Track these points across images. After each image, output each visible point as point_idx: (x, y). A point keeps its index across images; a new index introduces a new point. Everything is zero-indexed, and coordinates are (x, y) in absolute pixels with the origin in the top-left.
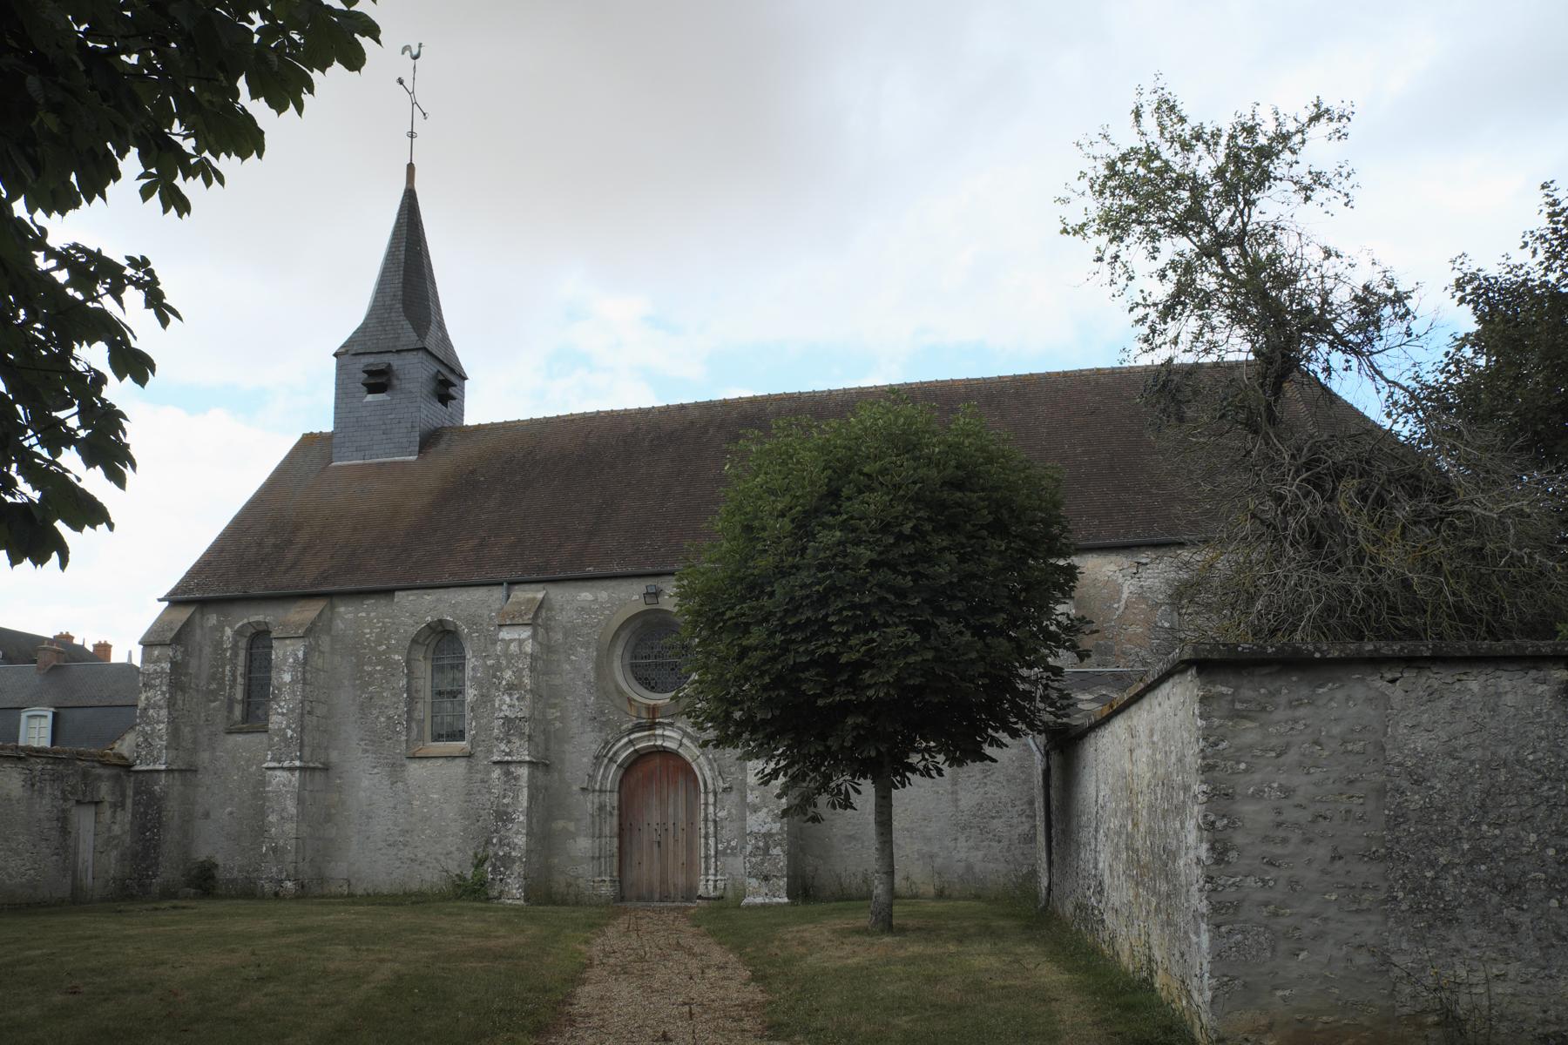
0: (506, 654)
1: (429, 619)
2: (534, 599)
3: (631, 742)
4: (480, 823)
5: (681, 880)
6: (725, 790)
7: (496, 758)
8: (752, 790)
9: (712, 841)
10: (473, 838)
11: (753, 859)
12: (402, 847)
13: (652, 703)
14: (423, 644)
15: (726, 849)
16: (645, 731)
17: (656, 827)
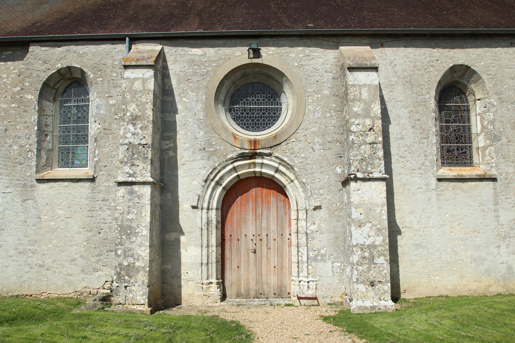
0: (130, 91)
1: (59, 66)
2: (153, 51)
3: (235, 169)
4: (100, 235)
5: (273, 280)
6: (316, 208)
7: (121, 179)
8: (356, 208)
9: (303, 250)
10: (95, 248)
11: (360, 268)
12: (31, 255)
13: (252, 138)
14: (53, 88)
15: (316, 256)
16: (246, 160)
17: (252, 237)
